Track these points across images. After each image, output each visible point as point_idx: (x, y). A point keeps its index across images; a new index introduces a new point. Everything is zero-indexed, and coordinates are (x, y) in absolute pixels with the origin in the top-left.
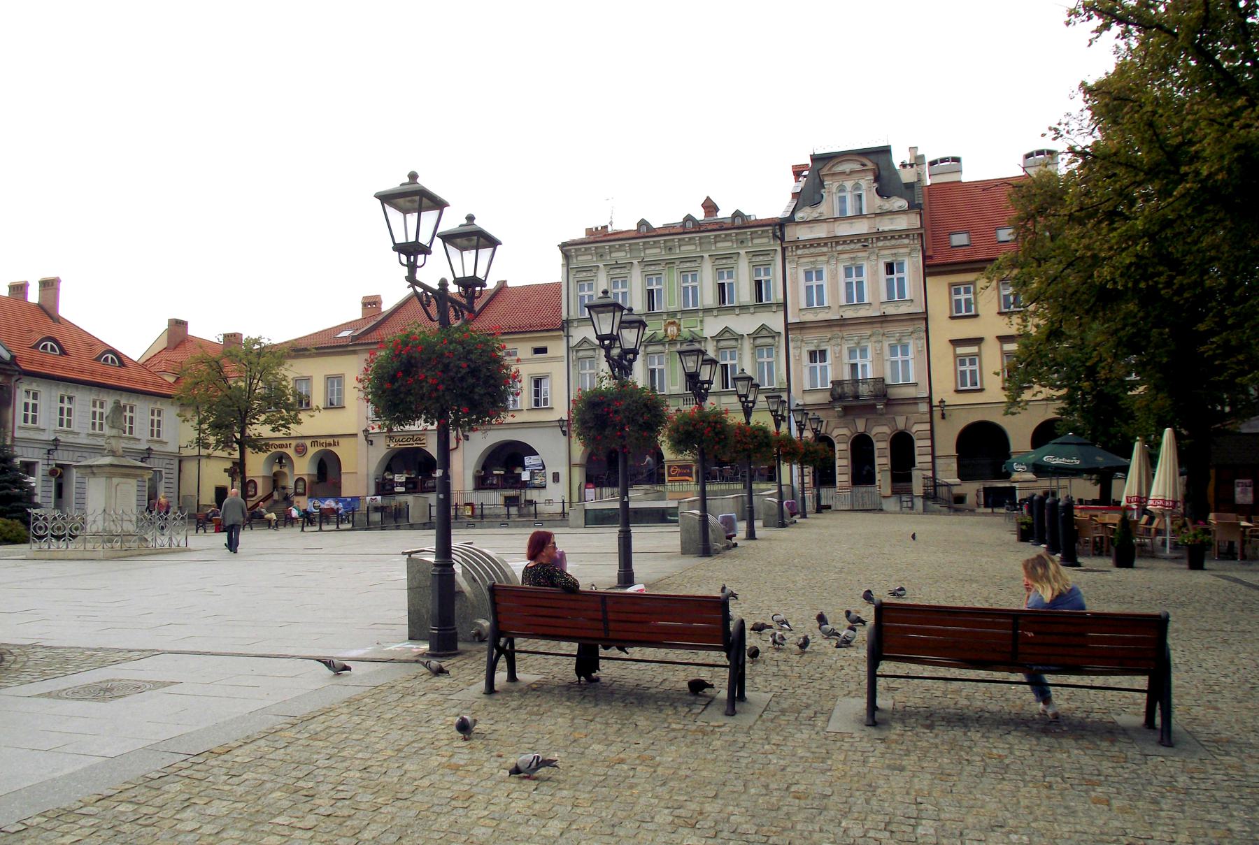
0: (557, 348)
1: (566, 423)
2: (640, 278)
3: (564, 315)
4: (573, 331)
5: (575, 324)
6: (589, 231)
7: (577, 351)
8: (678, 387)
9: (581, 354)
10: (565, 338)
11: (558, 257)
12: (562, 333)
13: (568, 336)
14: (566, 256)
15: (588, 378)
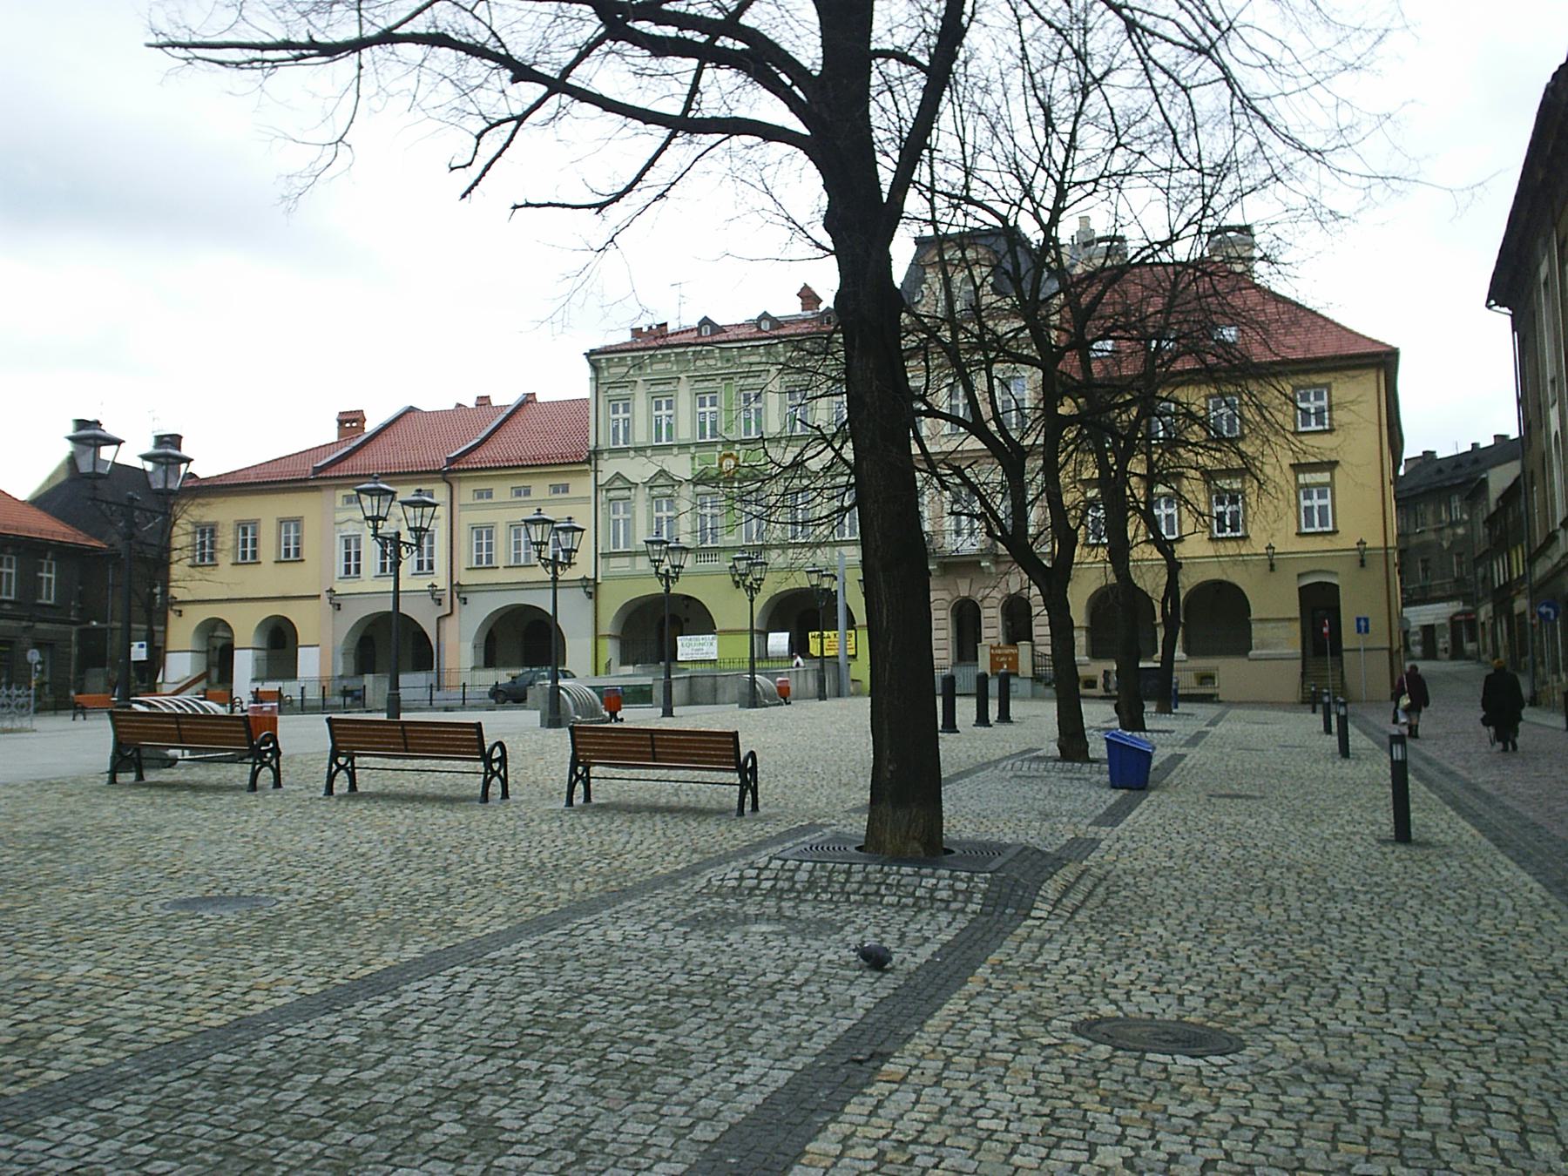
0: (582, 486)
1: (592, 583)
2: (688, 397)
3: (592, 443)
4: (602, 465)
5: (606, 455)
6: (637, 332)
7: (608, 490)
8: (734, 538)
9: (612, 494)
10: (593, 474)
11: (586, 370)
12: (587, 467)
13: (596, 471)
14: (595, 367)
15: (621, 526)
